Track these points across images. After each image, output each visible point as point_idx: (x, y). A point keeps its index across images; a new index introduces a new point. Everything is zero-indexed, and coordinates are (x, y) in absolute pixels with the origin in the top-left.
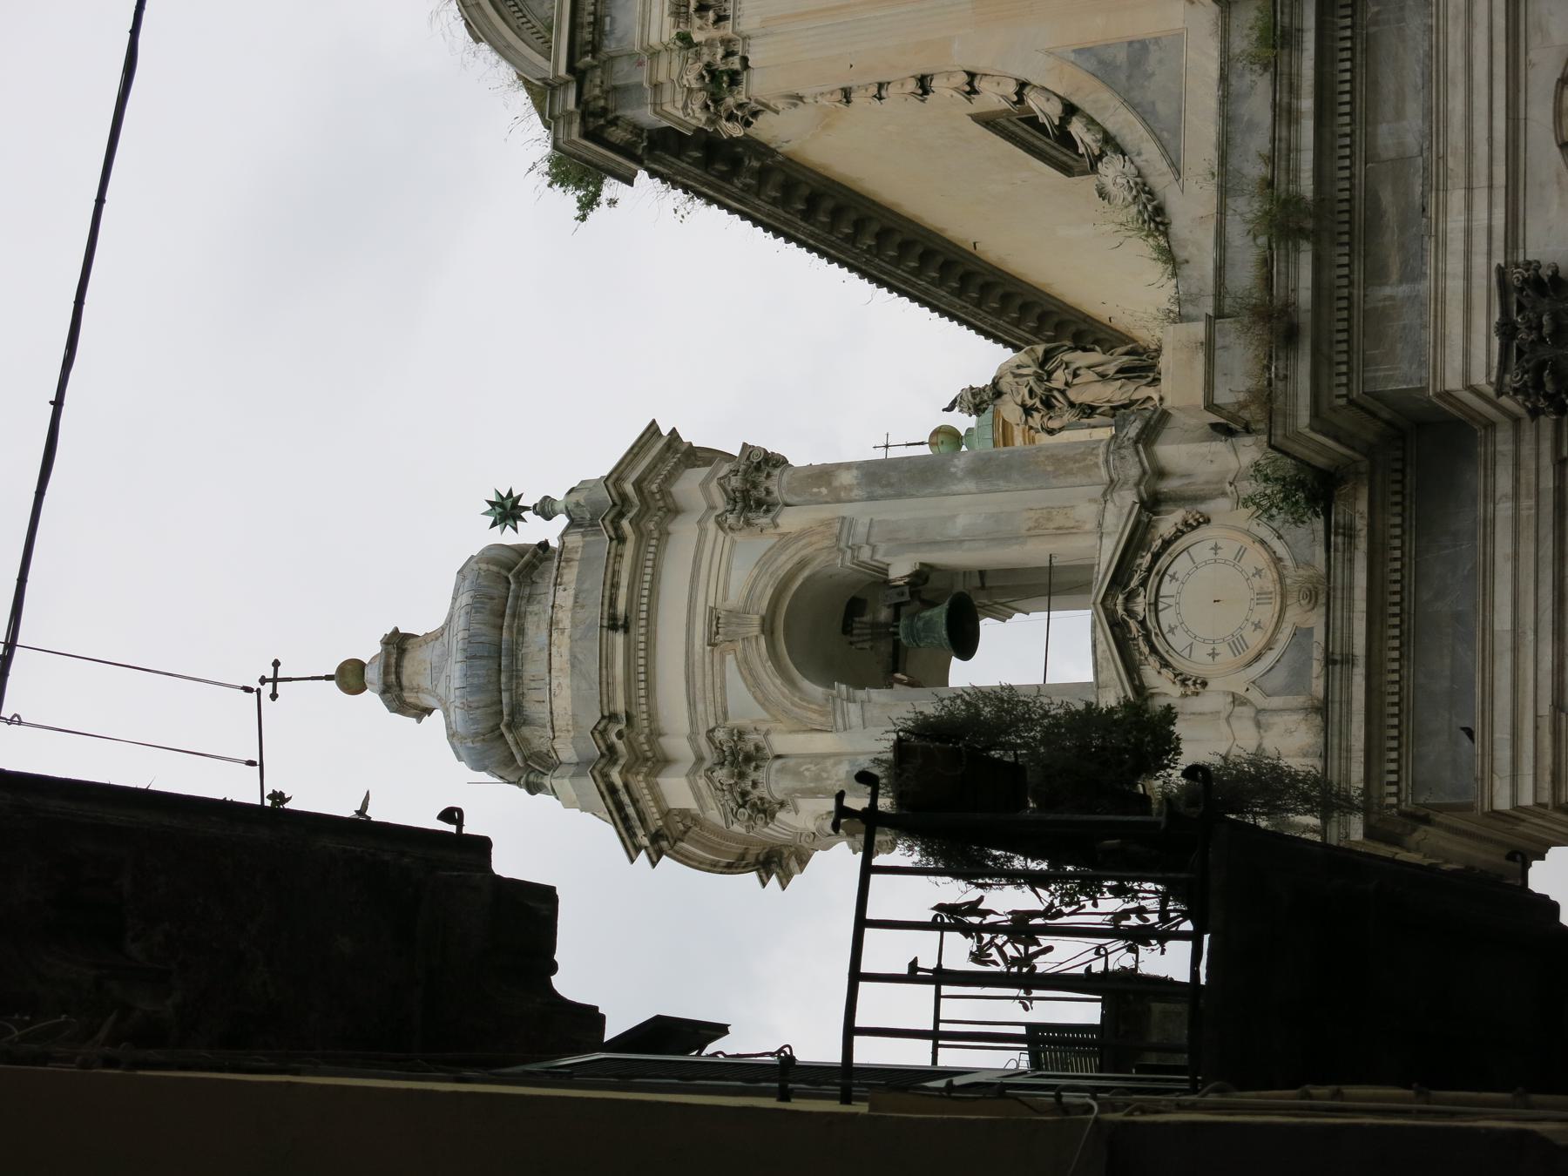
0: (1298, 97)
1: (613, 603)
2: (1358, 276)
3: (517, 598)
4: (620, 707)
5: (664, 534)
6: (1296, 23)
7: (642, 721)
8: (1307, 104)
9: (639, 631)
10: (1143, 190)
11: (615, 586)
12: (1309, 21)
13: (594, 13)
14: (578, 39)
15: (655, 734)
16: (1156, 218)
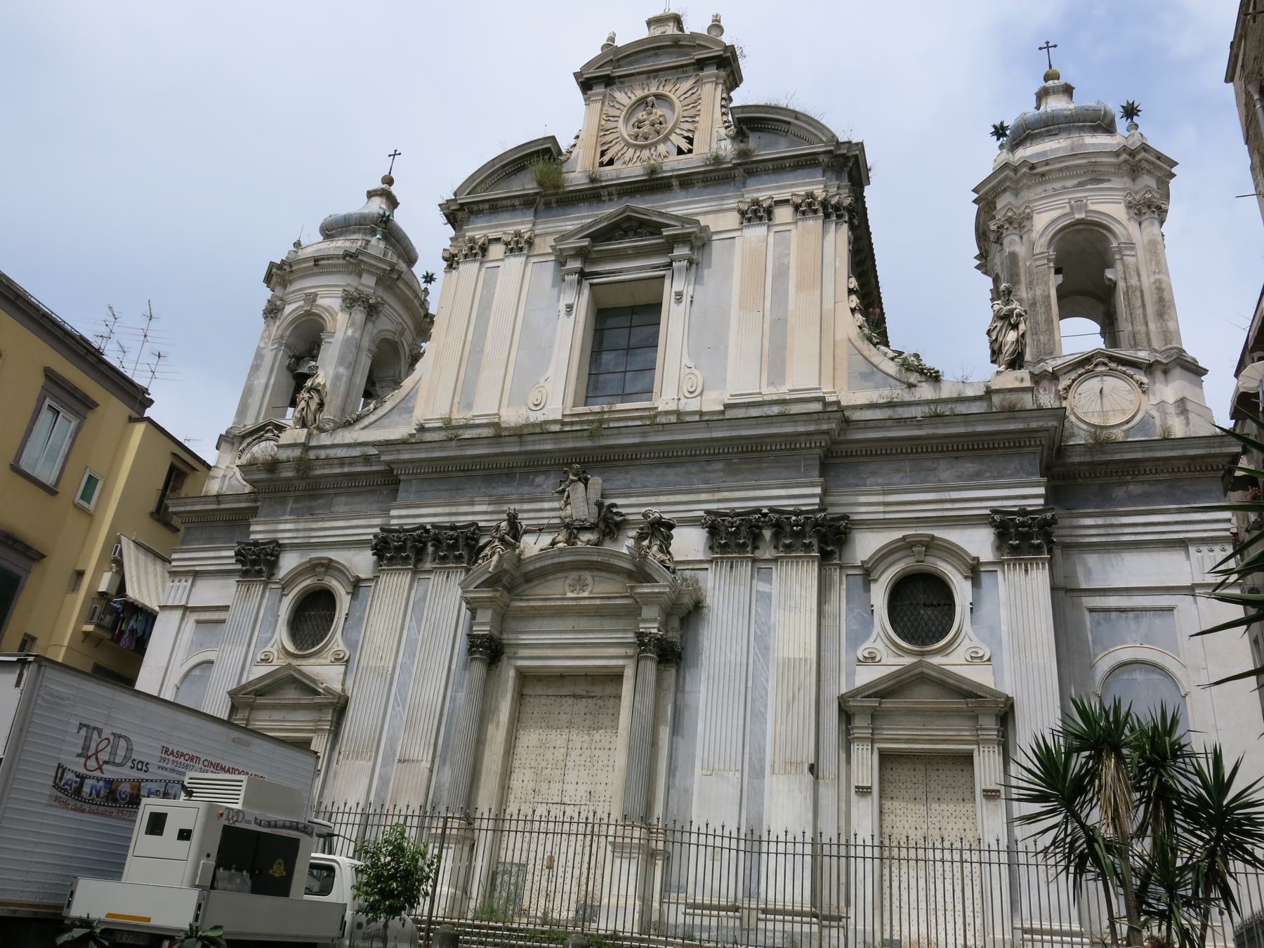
0: (349, 466)
1: (323, 259)
2: (297, 493)
3: (365, 229)
4: (294, 268)
5: (350, 273)
6: (373, 464)
7: (292, 277)
8: (346, 470)
9: (316, 270)
10: (359, 418)
11: (328, 259)
12: (374, 468)
13: (483, 210)
14: (473, 206)
15: (291, 282)
16: (348, 424)
